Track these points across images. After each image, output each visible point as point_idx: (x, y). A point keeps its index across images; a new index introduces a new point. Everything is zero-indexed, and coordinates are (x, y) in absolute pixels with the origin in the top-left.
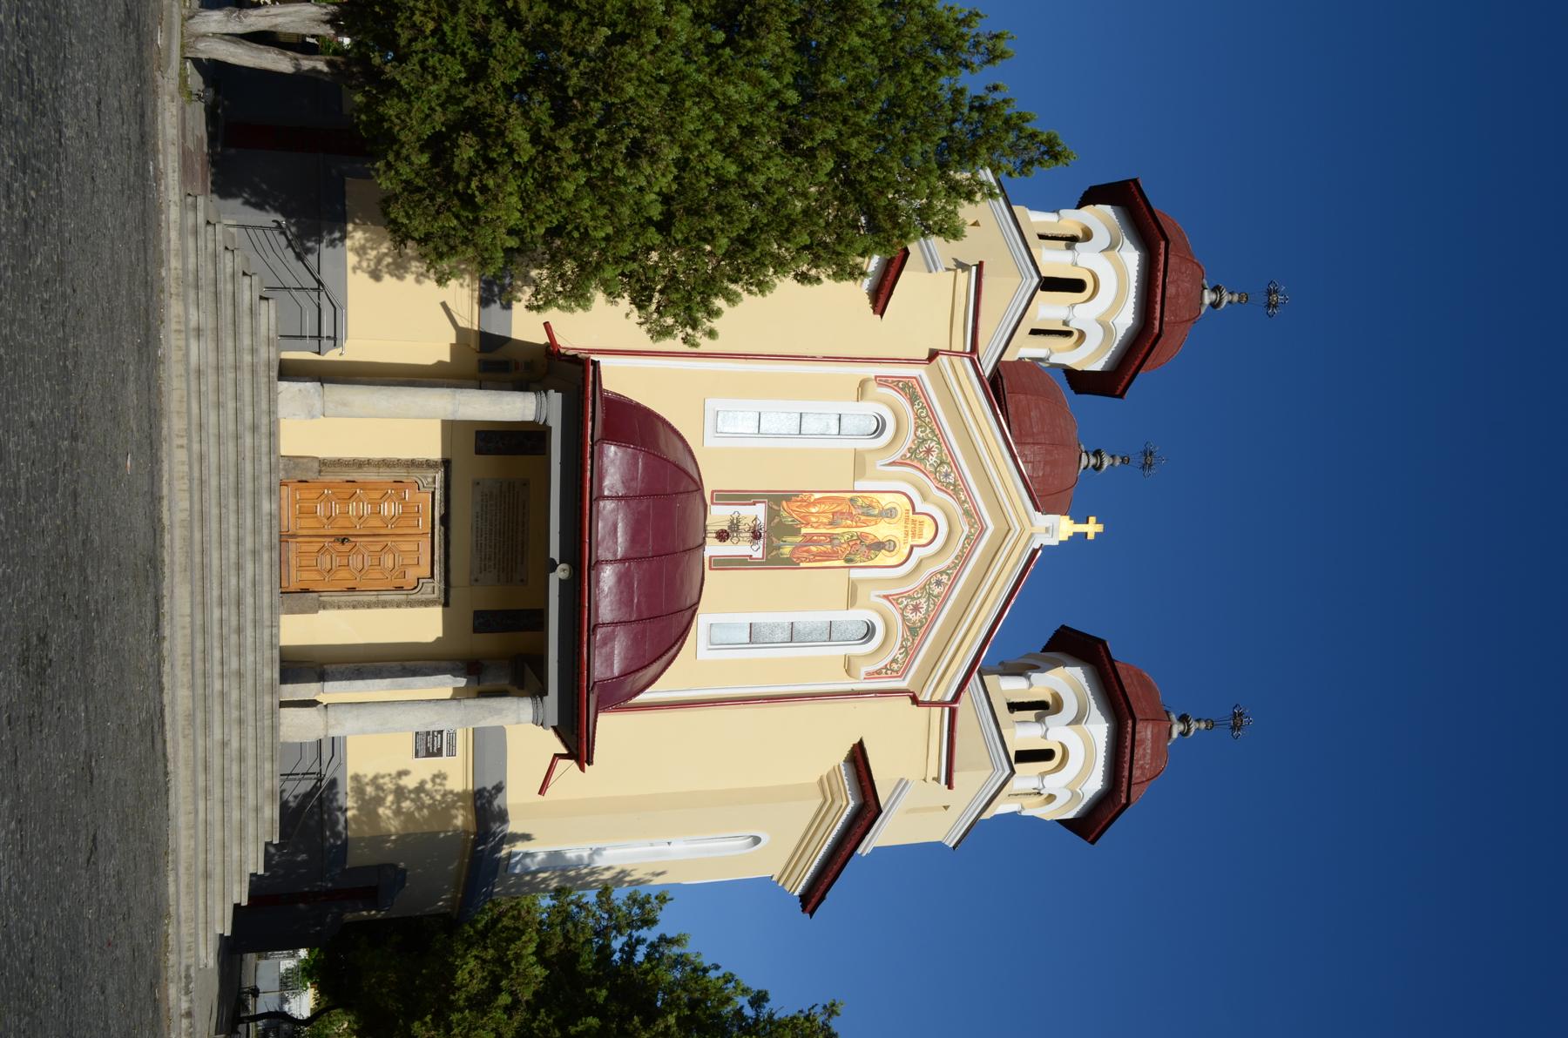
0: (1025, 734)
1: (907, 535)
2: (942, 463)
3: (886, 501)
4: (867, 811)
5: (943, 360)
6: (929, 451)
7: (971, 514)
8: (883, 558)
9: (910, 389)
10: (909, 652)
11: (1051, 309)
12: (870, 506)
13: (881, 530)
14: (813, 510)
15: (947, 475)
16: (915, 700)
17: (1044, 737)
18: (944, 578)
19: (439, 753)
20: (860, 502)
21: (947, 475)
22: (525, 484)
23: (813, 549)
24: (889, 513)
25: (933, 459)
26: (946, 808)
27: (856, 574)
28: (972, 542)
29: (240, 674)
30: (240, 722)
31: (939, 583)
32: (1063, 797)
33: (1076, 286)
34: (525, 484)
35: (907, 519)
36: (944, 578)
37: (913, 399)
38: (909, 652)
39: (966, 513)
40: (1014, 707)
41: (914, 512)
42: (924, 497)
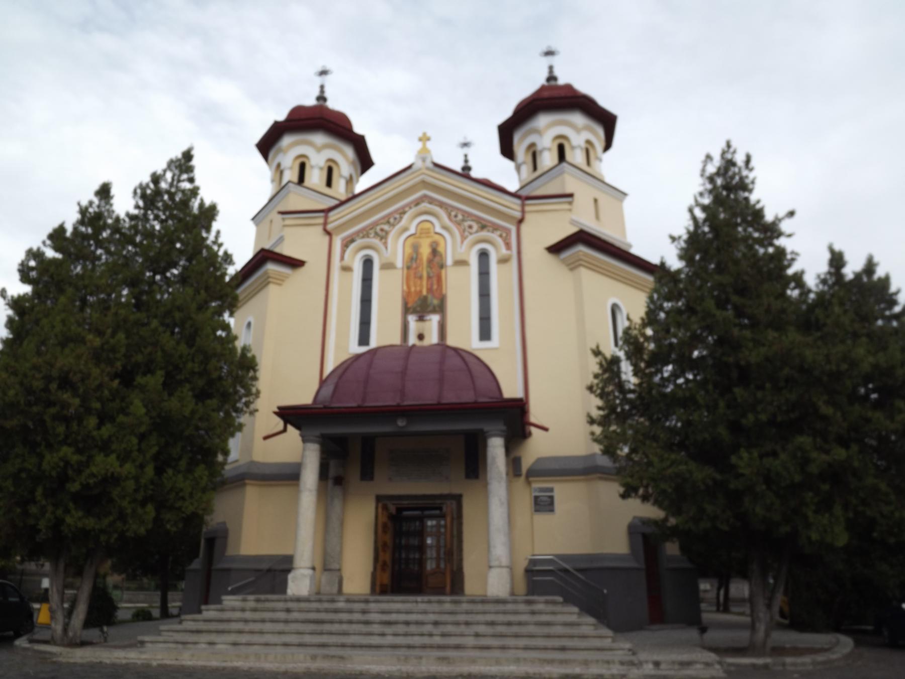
0: (548, 159)
1: (428, 237)
2: (388, 222)
3: (409, 250)
4: (583, 238)
5: (329, 227)
6: (382, 230)
7: (417, 203)
8: (441, 249)
9: (346, 245)
10: (496, 228)
11: (315, 178)
13: (425, 251)
15: (395, 219)
16: (521, 221)
17: (549, 149)
18: (453, 214)
19: (552, 498)
21: (395, 219)
24: (416, 248)
25: (386, 227)
26: (596, 201)
27: (449, 261)
28: (432, 201)
29: (436, 623)
30: (467, 624)
31: (456, 216)
32: (586, 135)
33: (302, 167)
35: (420, 237)
36: (453, 214)
37: (352, 241)
38: (496, 228)
40: (535, 168)
42: (406, 229)
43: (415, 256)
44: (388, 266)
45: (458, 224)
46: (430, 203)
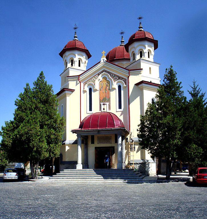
6: (93, 80)
14: (102, 96)
15: (97, 76)
21: (97, 76)
22: (98, 137)
25: (94, 79)
26: (150, 68)
28: (106, 71)
31: (112, 75)
34: (98, 137)
38: (122, 78)
39: (102, 73)
40: (134, 59)
45: (113, 77)
46: (105, 72)
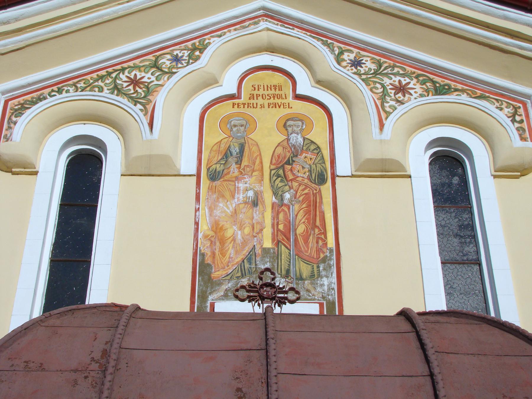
2: (156, 65)
3: (215, 136)
6: (135, 82)
12: (227, 154)
20: (219, 168)
21: (177, 59)
23: (301, 229)
25: (148, 77)
27: (344, 165)
41: (239, 97)
42: (212, 82)
43: (235, 150)
44: (149, 168)
